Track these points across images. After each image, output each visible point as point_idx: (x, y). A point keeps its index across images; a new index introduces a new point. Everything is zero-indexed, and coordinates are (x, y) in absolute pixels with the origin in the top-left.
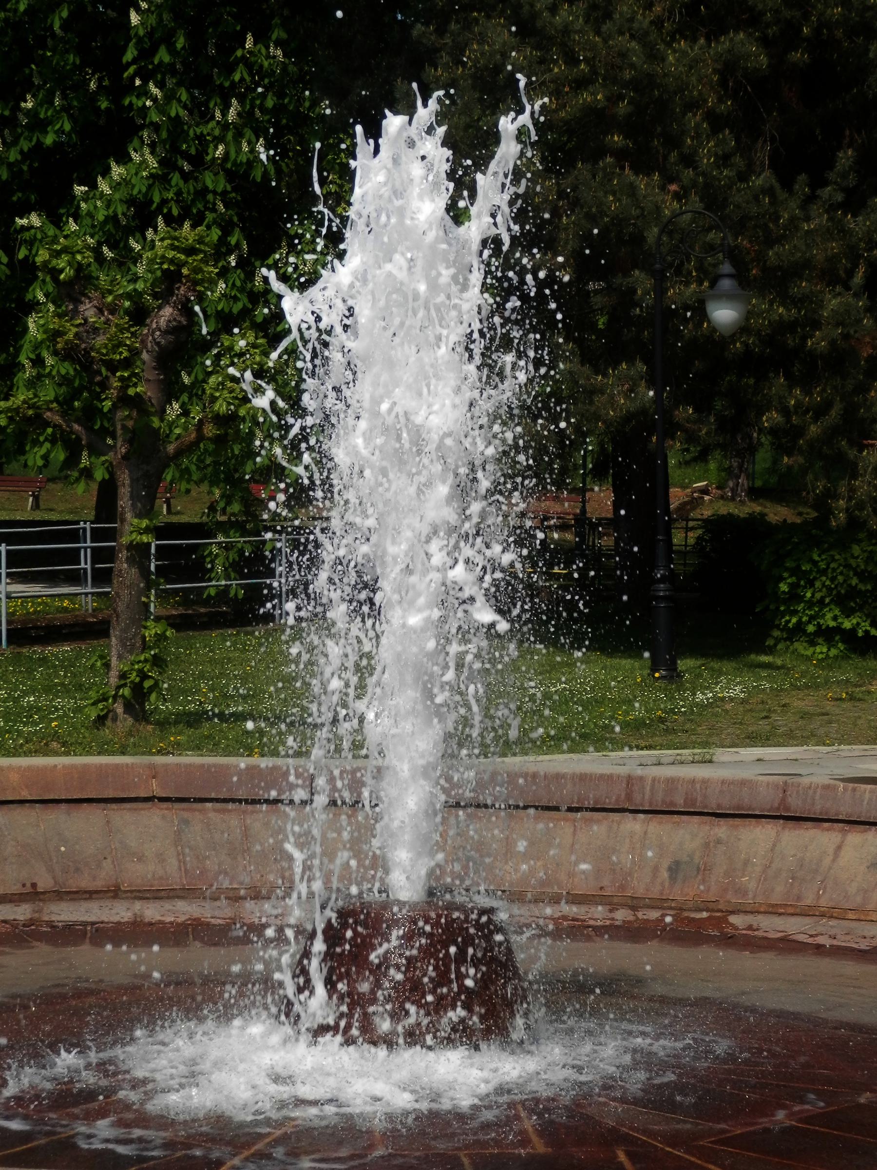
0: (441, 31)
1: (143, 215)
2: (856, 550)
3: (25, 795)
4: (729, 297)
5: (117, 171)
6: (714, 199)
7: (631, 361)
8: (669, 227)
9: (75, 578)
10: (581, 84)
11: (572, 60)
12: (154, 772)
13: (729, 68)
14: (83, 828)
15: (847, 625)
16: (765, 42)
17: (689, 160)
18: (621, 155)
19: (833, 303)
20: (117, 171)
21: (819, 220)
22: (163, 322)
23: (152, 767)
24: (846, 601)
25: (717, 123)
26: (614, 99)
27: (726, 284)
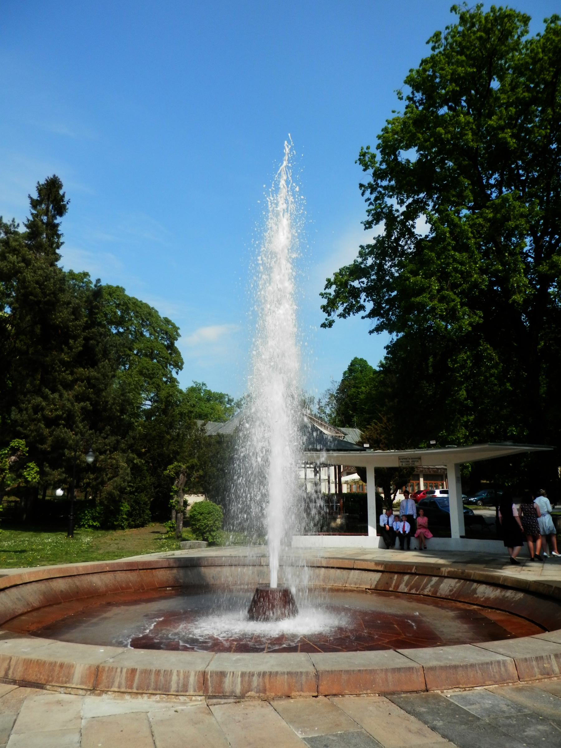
0: (25, 397)
2: (98, 508)
3: (83, 573)
4: (91, 456)
7: (61, 468)
8: (73, 440)
10: (56, 410)
11: (55, 405)
12: (107, 565)
15: (95, 524)
16: (91, 404)
18: (64, 426)
22: (13, 460)
23: (106, 564)
24: (94, 519)
26: (63, 413)
27: (91, 453)
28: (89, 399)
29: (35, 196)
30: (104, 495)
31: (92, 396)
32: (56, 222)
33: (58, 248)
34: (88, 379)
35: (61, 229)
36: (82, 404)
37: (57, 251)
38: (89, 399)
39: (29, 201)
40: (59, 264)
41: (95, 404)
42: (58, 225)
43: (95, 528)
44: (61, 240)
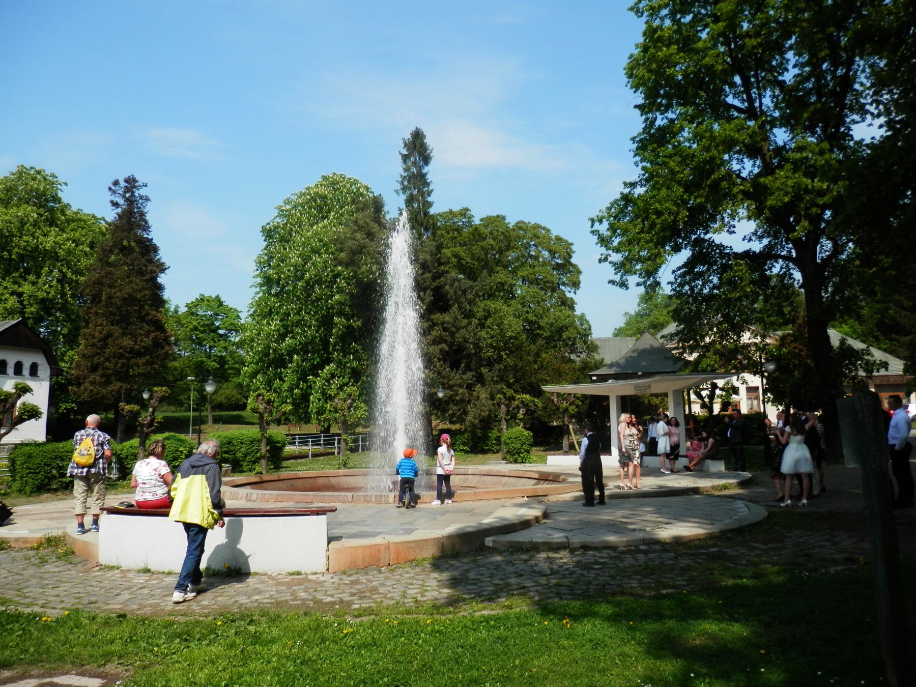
1: (333, 376)
5: (327, 368)
6: (439, 373)
9: (320, 445)
13: (441, 350)
14: (350, 479)
17: (435, 367)
19: (461, 391)
20: (327, 368)
21: (458, 376)
24: (464, 444)
25: (439, 360)
28: (445, 342)
29: (405, 152)
30: (467, 423)
31: (448, 338)
32: (424, 171)
33: (429, 195)
34: (443, 323)
35: (429, 178)
36: (440, 346)
37: (429, 199)
38: (445, 342)
39: (400, 157)
40: (432, 211)
41: (451, 345)
42: (425, 174)
43: (466, 452)
44: (431, 188)
